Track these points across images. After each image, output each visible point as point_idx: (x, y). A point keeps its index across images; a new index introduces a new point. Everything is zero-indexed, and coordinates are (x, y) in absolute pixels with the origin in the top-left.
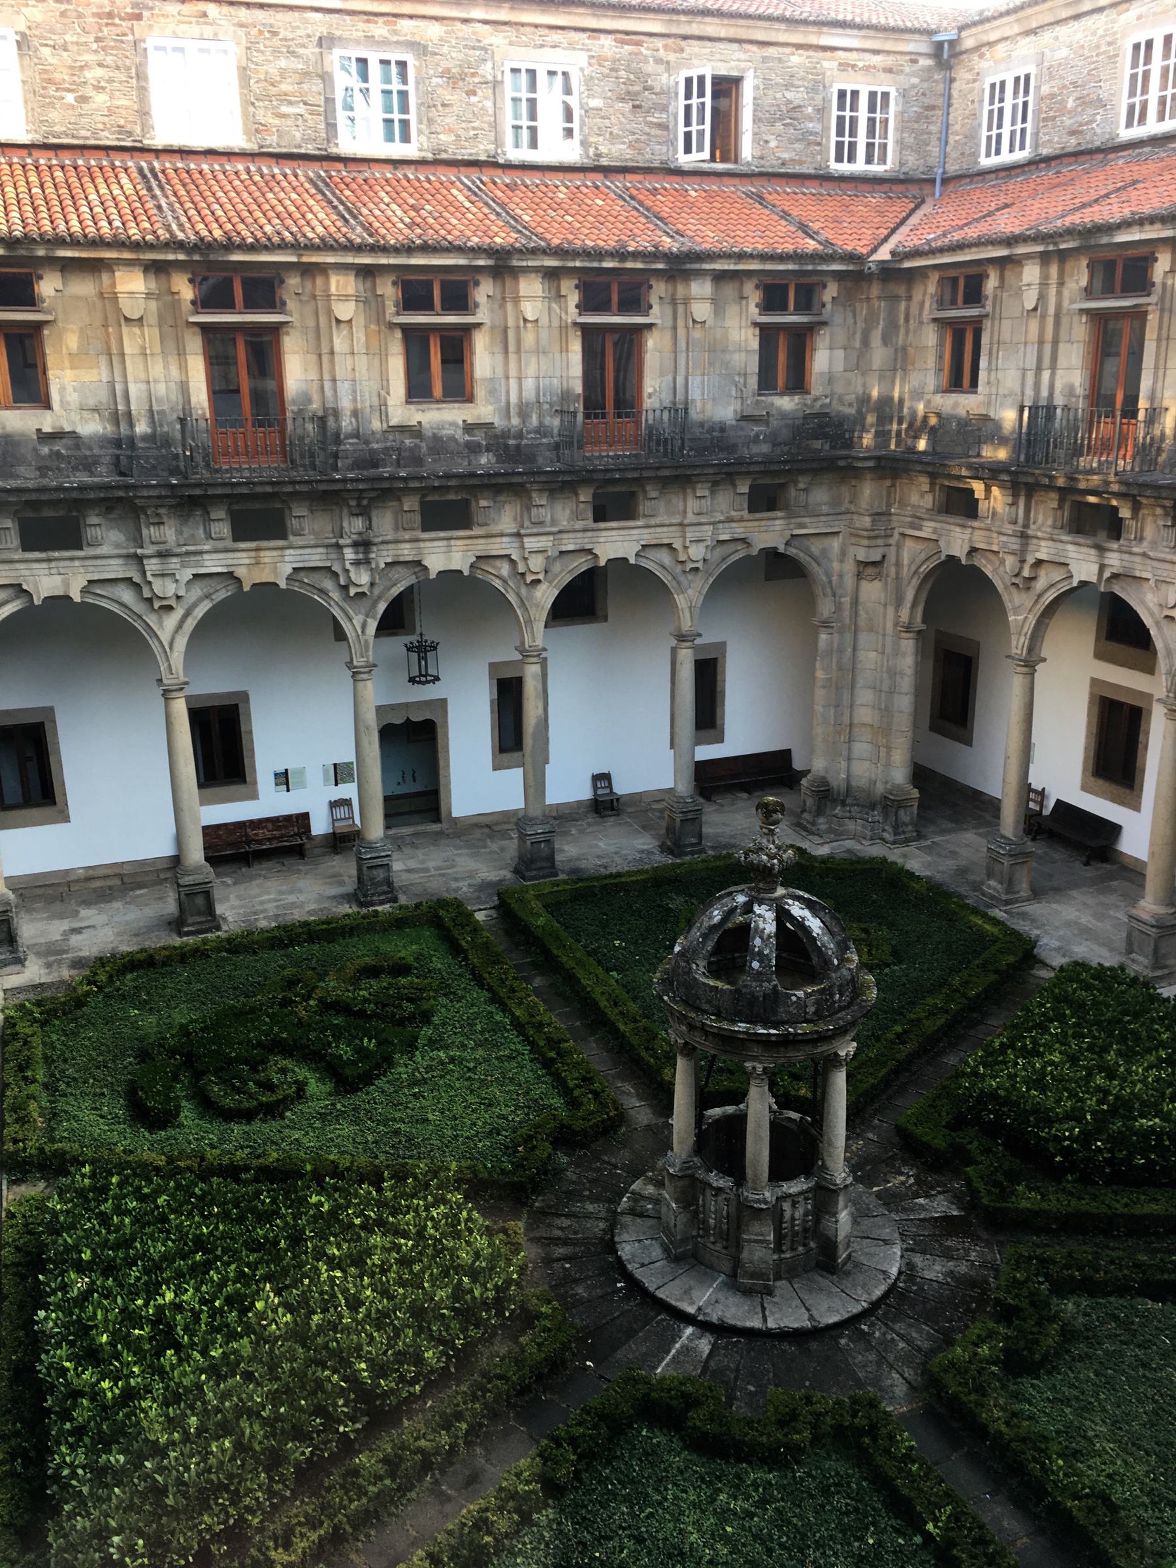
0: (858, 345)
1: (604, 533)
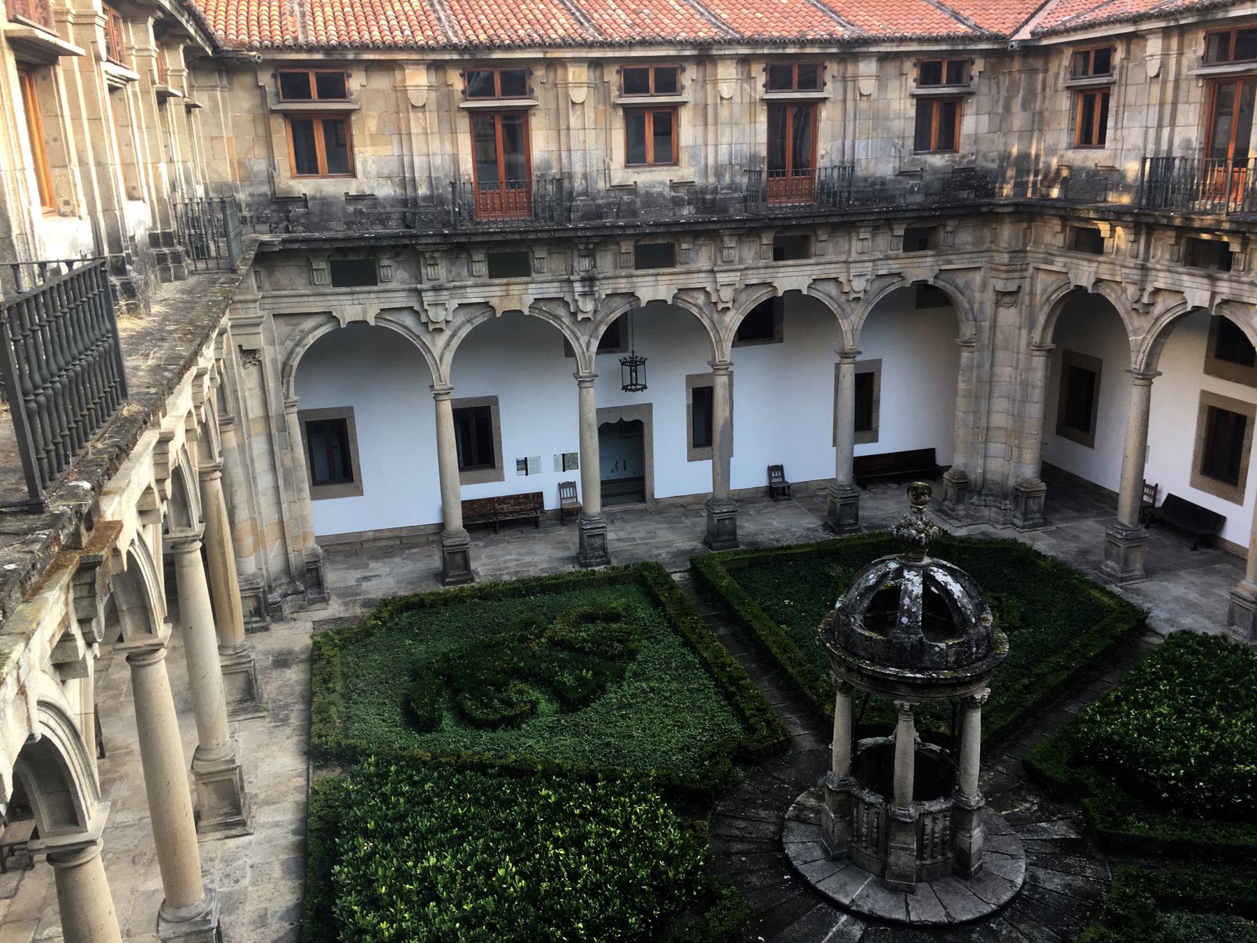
0: (1000, 110)
1: (782, 270)
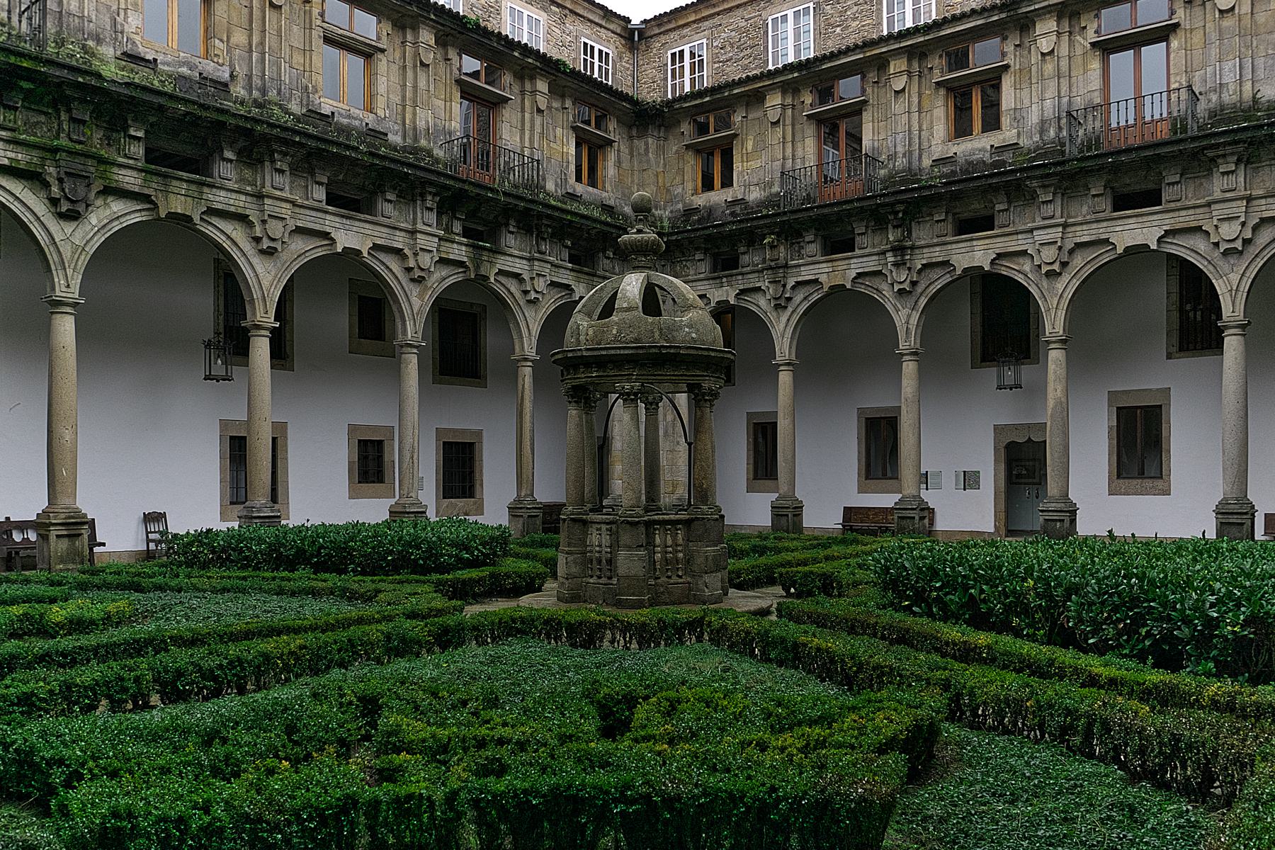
1: (1120, 222)
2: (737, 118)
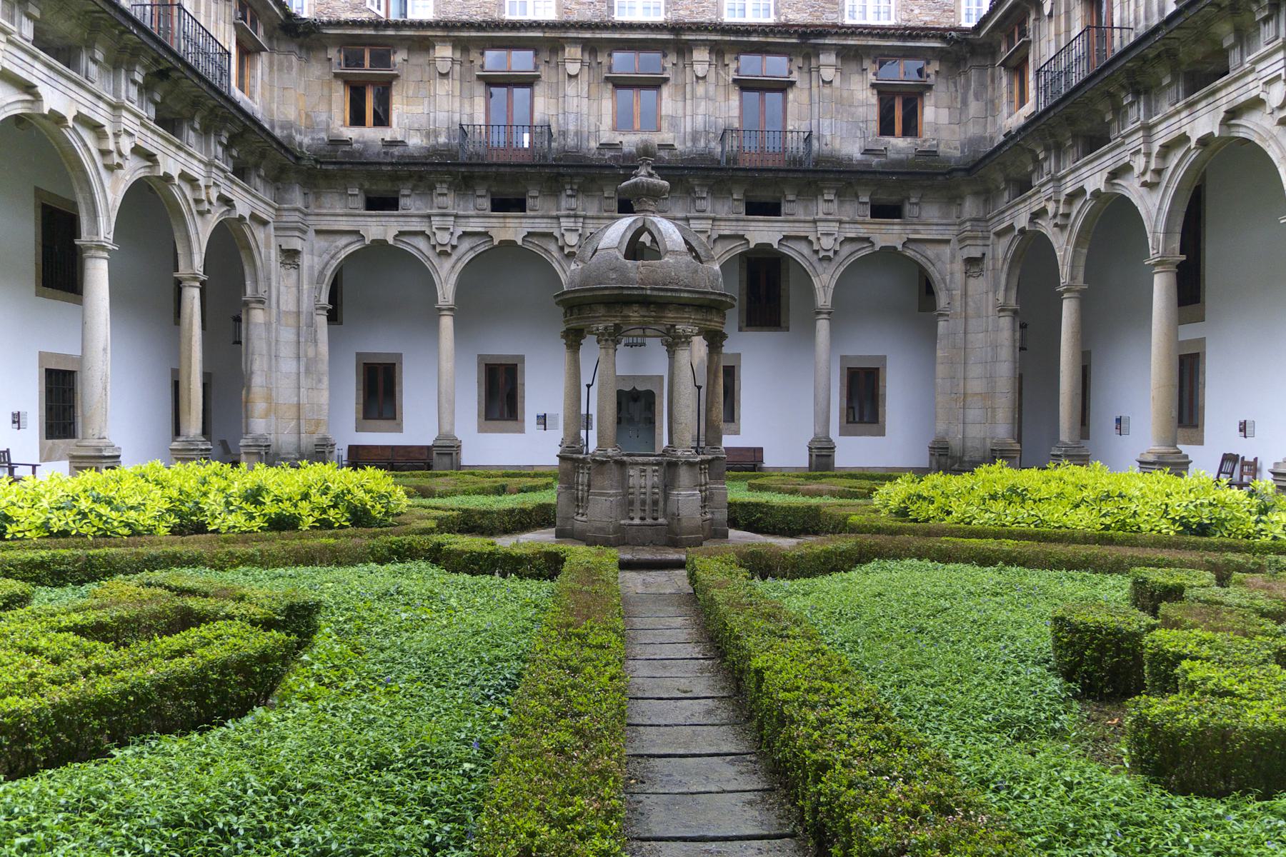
2: (398, 57)
